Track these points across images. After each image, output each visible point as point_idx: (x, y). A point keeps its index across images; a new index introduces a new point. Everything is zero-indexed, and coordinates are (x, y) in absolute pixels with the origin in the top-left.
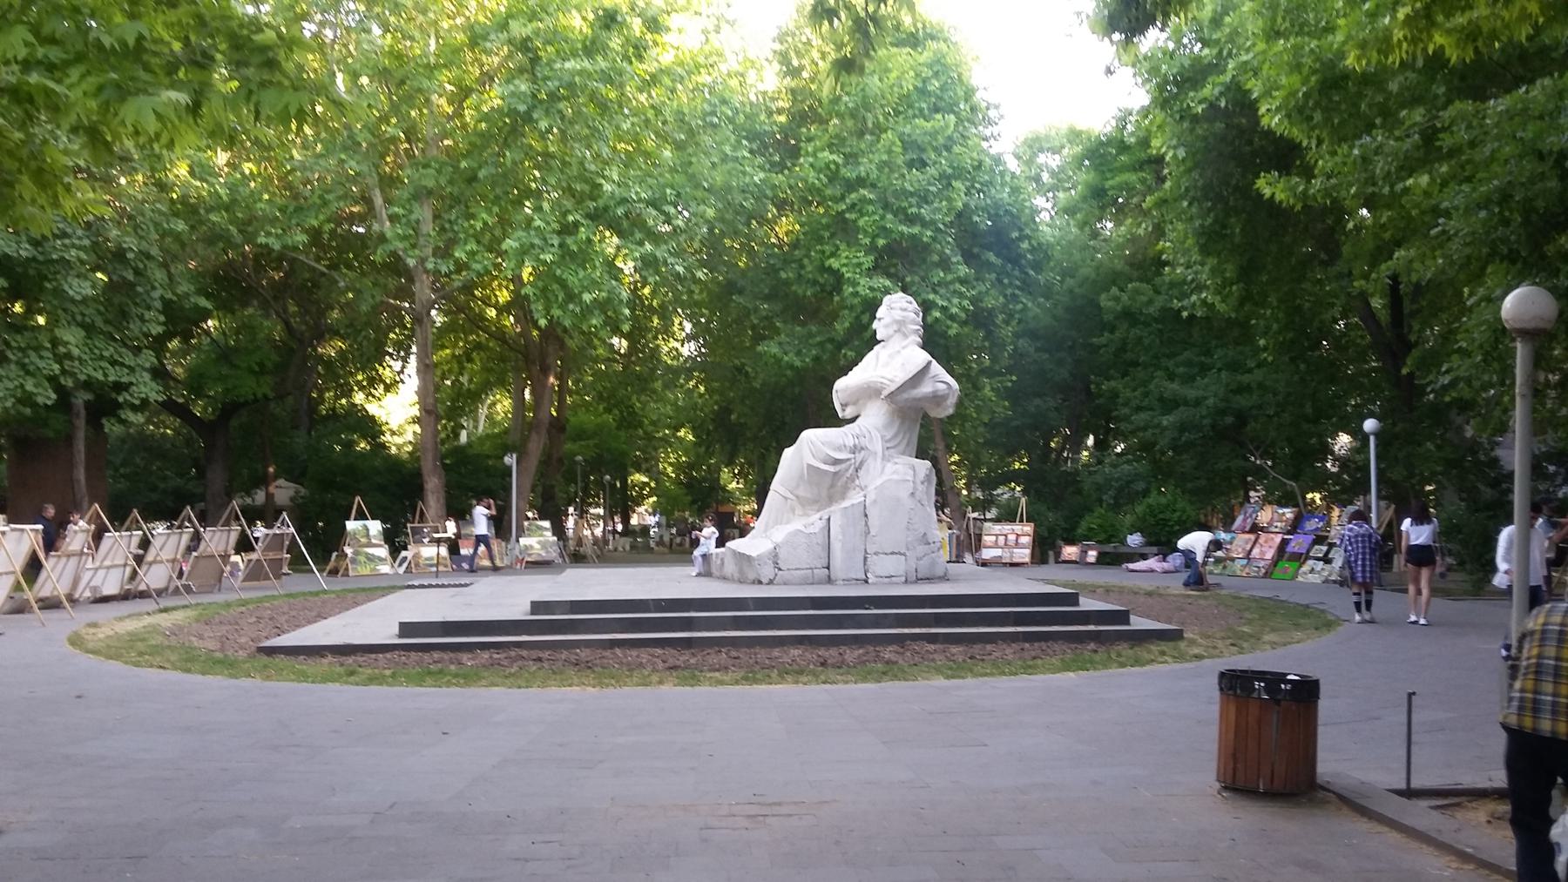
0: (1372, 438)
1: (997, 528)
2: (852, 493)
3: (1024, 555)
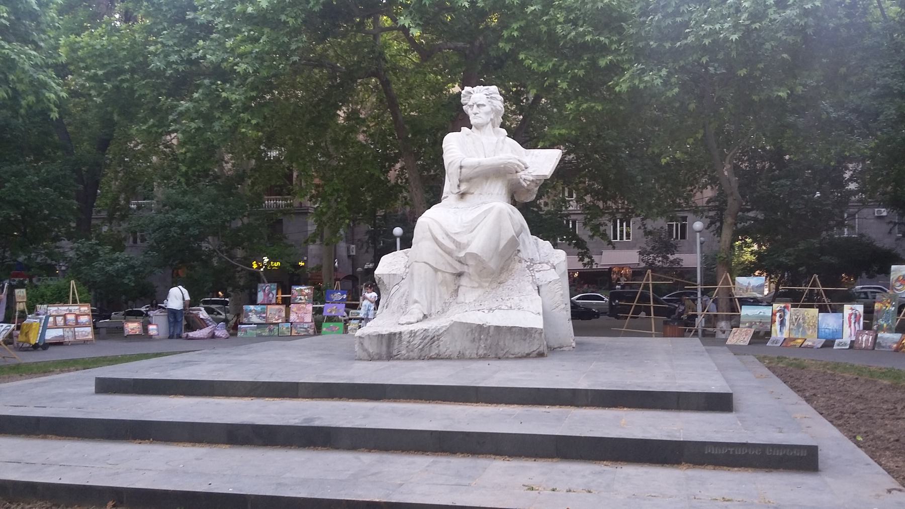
0: (398, 240)
1: (53, 309)
2: (518, 266)
3: (86, 332)
